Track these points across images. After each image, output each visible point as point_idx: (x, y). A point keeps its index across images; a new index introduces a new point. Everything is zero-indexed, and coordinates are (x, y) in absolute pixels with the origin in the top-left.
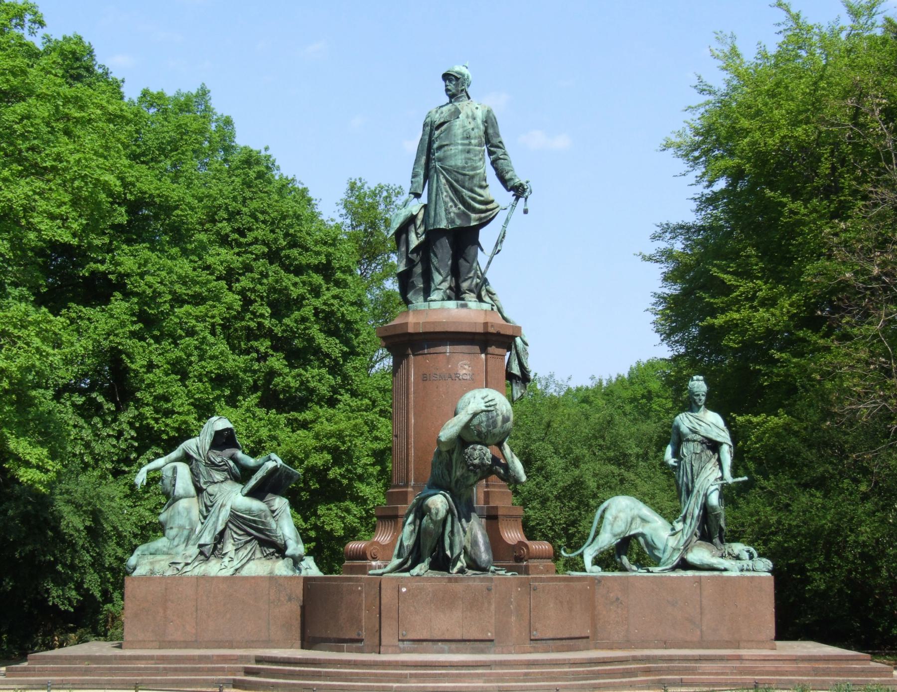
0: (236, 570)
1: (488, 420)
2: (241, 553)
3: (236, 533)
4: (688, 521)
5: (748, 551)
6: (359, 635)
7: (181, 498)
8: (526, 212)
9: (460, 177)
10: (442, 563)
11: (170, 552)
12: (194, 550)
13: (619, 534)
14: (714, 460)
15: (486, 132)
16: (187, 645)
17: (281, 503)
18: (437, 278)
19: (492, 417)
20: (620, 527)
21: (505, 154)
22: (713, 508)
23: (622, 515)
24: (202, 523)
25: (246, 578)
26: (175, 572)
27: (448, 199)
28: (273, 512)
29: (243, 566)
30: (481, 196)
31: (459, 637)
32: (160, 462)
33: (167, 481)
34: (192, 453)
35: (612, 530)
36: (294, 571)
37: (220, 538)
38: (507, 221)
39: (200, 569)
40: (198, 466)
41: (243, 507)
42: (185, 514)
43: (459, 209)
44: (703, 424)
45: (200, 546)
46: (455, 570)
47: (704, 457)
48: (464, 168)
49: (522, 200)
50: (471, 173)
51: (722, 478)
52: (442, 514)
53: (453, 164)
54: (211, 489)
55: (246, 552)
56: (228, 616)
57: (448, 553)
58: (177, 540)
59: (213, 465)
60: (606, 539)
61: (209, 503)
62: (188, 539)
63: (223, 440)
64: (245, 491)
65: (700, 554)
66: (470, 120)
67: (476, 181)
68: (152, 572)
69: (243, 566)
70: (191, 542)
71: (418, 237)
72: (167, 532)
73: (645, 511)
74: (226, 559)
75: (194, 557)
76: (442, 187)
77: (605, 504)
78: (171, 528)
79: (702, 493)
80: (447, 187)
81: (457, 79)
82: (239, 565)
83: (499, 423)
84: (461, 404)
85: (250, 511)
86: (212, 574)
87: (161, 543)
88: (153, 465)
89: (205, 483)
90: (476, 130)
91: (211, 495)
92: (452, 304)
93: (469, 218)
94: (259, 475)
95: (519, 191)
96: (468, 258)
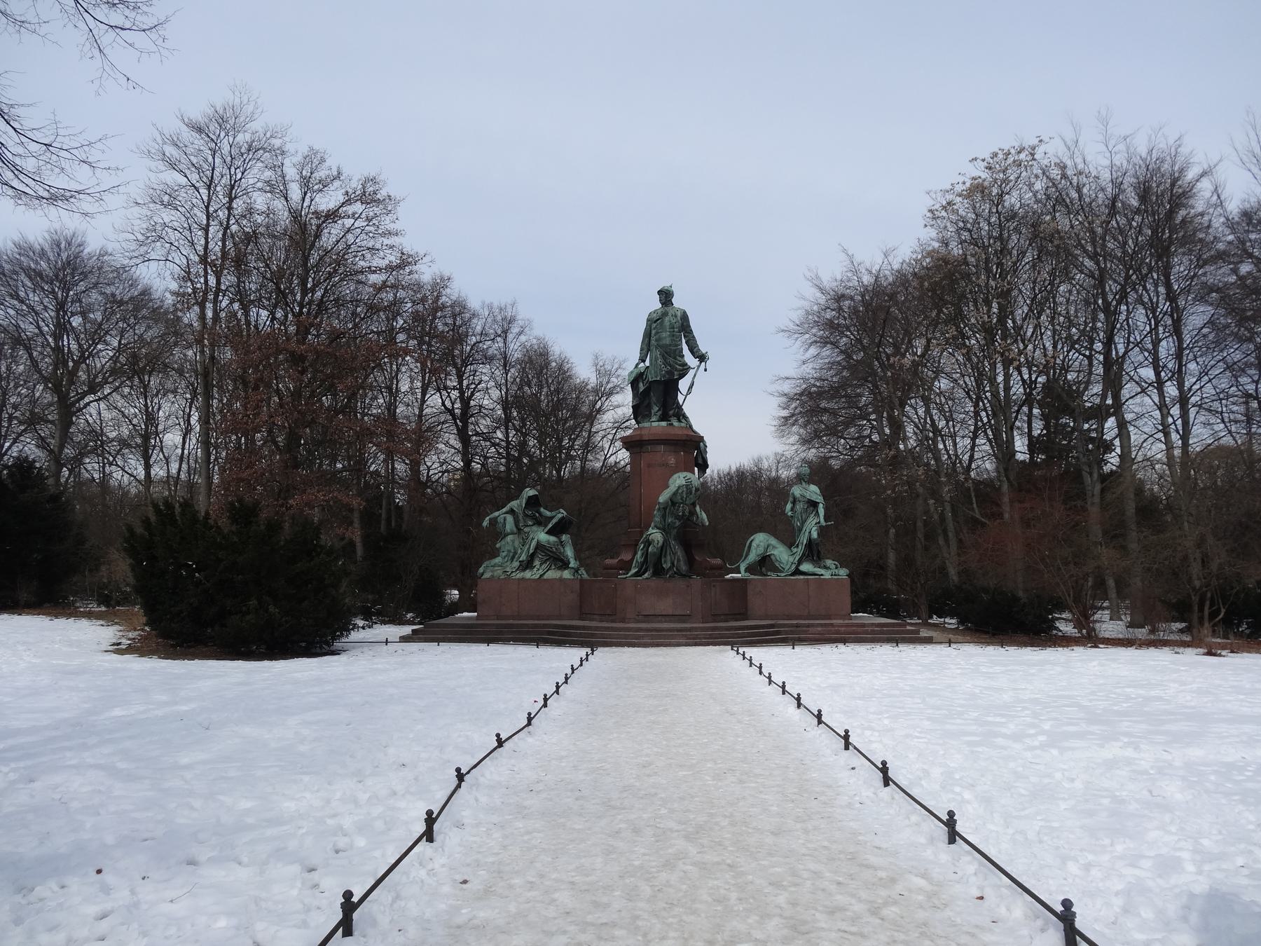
4: (800, 547)
7: (508, 534)
8: (706, 370)
10: (658, 572)
12: (516, 564)
15: (682, 324)
16: (513, 618)
20: (760, 551)
21: (694, 337)
25: (547, 580)
31: (671, 613)
32: (496, 514)
36: (574, 576)
37: (532, 557)
38: (695, 375)
39: (520, 575)
40: (518, 517)
48: (670, 345)
49: (703, 363)
51: (819, 523)
52: (660, 544)
57: (664, 566)
59: (527, 516)
60: (753, 557)
63: (533, 502)
64: (546, 530)
65: (806, 567)
67: (677, 352)
68: (492, 576)
73: (773, 541)
74: (535, 569)
77: (752, 538)
79: (808, 531)
84: (671, 481)
85: (548, 542)
87: (498, 560)
88: (492, 516)
92: (664, 424)
94: (554, 521)
95: (702, 358)
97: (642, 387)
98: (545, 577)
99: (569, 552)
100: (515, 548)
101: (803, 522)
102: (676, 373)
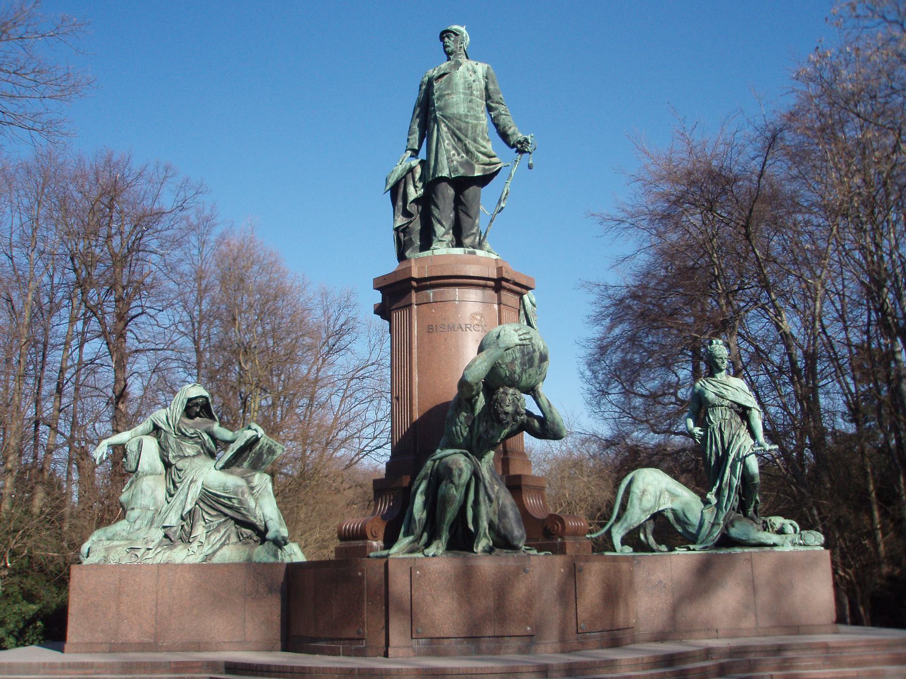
0: (208, 557)
1: (523, 355)
2: (212, 538)
3: (207, 513)
5: (791, 524)
6: (359, 633)
9: (463, 125)
11: (130, 536)
13: (649, 510)
14: (744, 428)
15: (487, 89)
16: (143, 647)
17: (261, 480)
18: (439, 230)
19: (528, 353)
22: (752, 477)
23: (651, 489)
24: (168, 503)
26: (133, 559)
27: (450, 147)
28: (252, 488)
29: (215, 552)
30: (485, 147)
33: (131, 457)
34: (161, 425)
35: (640, 504)
37: (189, 517)
40: (166, 439)
41: (216, 484)
42: (150, 493)
43: (462, 157)
44: (729, 388)
45: (164, 527)
46: (480, 548)
47: (734, 424)
48: (466, 116)
50: (475, 122)
53: (456, 112)
54: (180, 465)
55: (218, 536)
56: (195, 611)
58: (138, 522)
61: (177, 479)
62: (152, 522)
64: (221, 464)
66: (471, 73)
69: (215, 552)
70: (155, 525)
71: (416, 191)
72: (128, 512)
74: (195, 545)
75: (157, 541)
76: (444, 135)
77: (629, 477)
78: (133, 509)
80: (449, 135)
81: (456, 35)
82: (210, 551)
83: (537, 361)
85: (225, 489)
86: (178, 561)
87: (121, 527)
89: (174, 457)
90: (477, 83)
91: (180, 470)
93: (473, 169)
96: (472, 213)
100: (155, 504)
102: (477, 166)
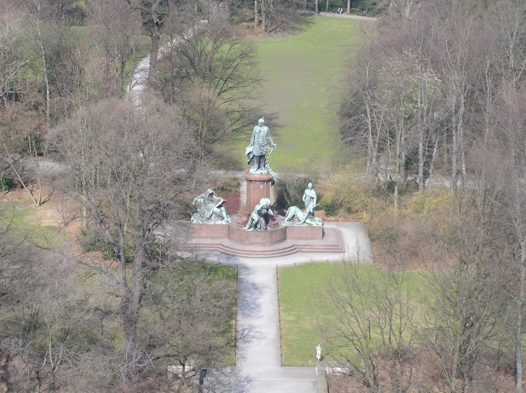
20: (293, 214)
60: (290, 216)
97: (251, 156)
98: (216, 223)
99: (224, 214)
101: (308, 204)
